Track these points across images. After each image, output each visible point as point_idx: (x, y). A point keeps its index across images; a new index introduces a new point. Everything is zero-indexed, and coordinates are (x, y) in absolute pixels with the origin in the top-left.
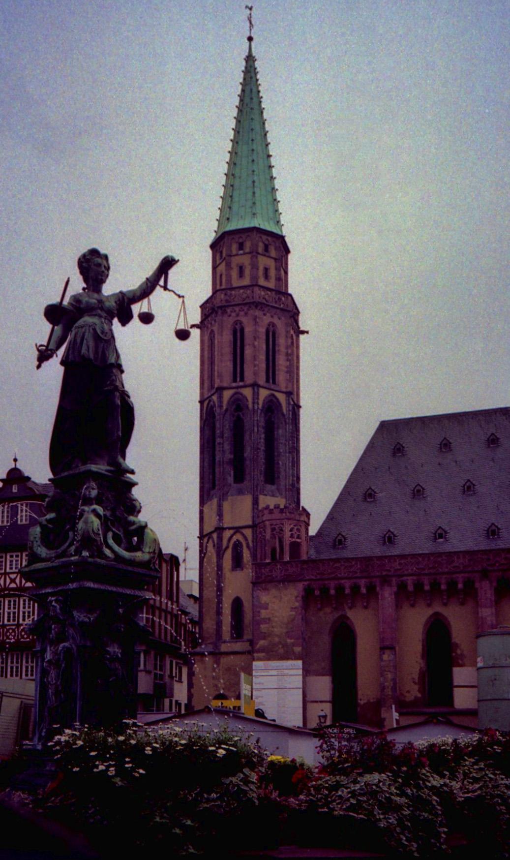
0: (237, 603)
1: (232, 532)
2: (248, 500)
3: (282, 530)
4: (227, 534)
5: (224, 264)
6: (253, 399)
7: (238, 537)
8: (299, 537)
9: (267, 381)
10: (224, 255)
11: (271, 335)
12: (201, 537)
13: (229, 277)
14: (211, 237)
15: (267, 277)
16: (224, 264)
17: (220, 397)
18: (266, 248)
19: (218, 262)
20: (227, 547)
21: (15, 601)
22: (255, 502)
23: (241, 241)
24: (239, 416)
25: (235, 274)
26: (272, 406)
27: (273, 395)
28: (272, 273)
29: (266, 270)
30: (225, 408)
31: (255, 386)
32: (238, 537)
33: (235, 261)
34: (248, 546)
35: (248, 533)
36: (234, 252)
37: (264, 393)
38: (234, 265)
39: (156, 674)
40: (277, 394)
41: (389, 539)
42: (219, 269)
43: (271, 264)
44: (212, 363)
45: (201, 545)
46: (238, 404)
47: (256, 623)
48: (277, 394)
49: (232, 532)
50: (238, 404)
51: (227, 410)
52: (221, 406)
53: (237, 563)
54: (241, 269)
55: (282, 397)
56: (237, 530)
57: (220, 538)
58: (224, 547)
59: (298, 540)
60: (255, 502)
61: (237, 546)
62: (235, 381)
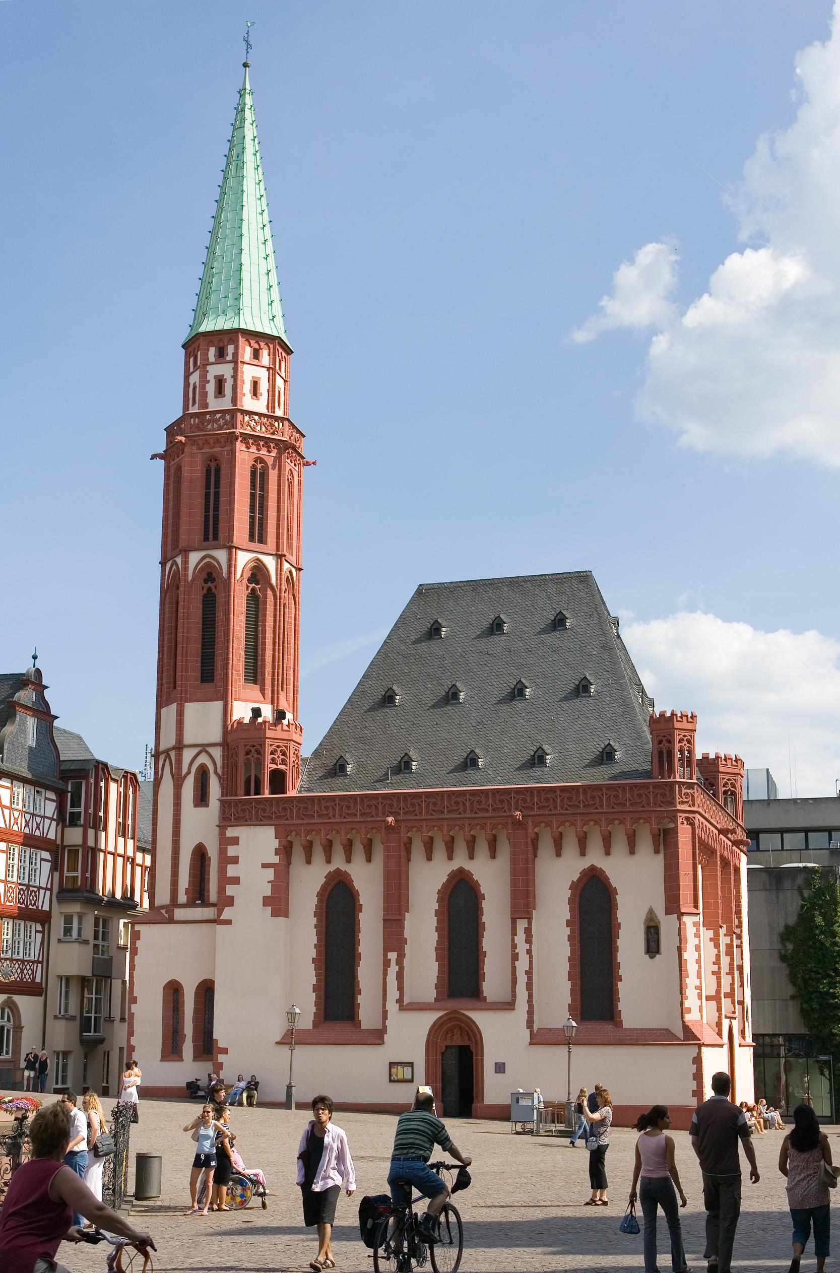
0: (200, 854)
1: (195, 751)
4: (188, 754)
5: (197, 373)
6: (229, 566)
8: (283, 762)
9: (252, 538)
11: (259, 477)
12: (156, 755)
13: (204, 394)
14: (184, 335)
15: (255, 392)
16: (197, 373)
17: (186, 563)
18: (256, 354)
19: (191, 370)
20: (189, 773)
22: (226, 712)
23: (221, 345)
24: (209, 589)
25: (211, 388)
26: (258, 573)
27: (258, 559)
28: (264, 387)
29: (255, 384)
30: (190, 577)
32: (203, 759)
33: (214, 371)
34: (216, 772)
35: (217, 753)
36: (212, 359)
37: (243, 559)
38: (210, 377)
39: (95, 946)
40: (263, 558)
43: (263, 375)
44: (177, 515)
47: (225, 880)
48: (263, 558)
49: (195, 751)
52: (186, 575)
53: (202, 799)
54: (220, 382)
55: (270, 563)
56: (203, 748)
57: (179, 761)
58: (185, 770)
59: (283, 767)
62: (206, 539)
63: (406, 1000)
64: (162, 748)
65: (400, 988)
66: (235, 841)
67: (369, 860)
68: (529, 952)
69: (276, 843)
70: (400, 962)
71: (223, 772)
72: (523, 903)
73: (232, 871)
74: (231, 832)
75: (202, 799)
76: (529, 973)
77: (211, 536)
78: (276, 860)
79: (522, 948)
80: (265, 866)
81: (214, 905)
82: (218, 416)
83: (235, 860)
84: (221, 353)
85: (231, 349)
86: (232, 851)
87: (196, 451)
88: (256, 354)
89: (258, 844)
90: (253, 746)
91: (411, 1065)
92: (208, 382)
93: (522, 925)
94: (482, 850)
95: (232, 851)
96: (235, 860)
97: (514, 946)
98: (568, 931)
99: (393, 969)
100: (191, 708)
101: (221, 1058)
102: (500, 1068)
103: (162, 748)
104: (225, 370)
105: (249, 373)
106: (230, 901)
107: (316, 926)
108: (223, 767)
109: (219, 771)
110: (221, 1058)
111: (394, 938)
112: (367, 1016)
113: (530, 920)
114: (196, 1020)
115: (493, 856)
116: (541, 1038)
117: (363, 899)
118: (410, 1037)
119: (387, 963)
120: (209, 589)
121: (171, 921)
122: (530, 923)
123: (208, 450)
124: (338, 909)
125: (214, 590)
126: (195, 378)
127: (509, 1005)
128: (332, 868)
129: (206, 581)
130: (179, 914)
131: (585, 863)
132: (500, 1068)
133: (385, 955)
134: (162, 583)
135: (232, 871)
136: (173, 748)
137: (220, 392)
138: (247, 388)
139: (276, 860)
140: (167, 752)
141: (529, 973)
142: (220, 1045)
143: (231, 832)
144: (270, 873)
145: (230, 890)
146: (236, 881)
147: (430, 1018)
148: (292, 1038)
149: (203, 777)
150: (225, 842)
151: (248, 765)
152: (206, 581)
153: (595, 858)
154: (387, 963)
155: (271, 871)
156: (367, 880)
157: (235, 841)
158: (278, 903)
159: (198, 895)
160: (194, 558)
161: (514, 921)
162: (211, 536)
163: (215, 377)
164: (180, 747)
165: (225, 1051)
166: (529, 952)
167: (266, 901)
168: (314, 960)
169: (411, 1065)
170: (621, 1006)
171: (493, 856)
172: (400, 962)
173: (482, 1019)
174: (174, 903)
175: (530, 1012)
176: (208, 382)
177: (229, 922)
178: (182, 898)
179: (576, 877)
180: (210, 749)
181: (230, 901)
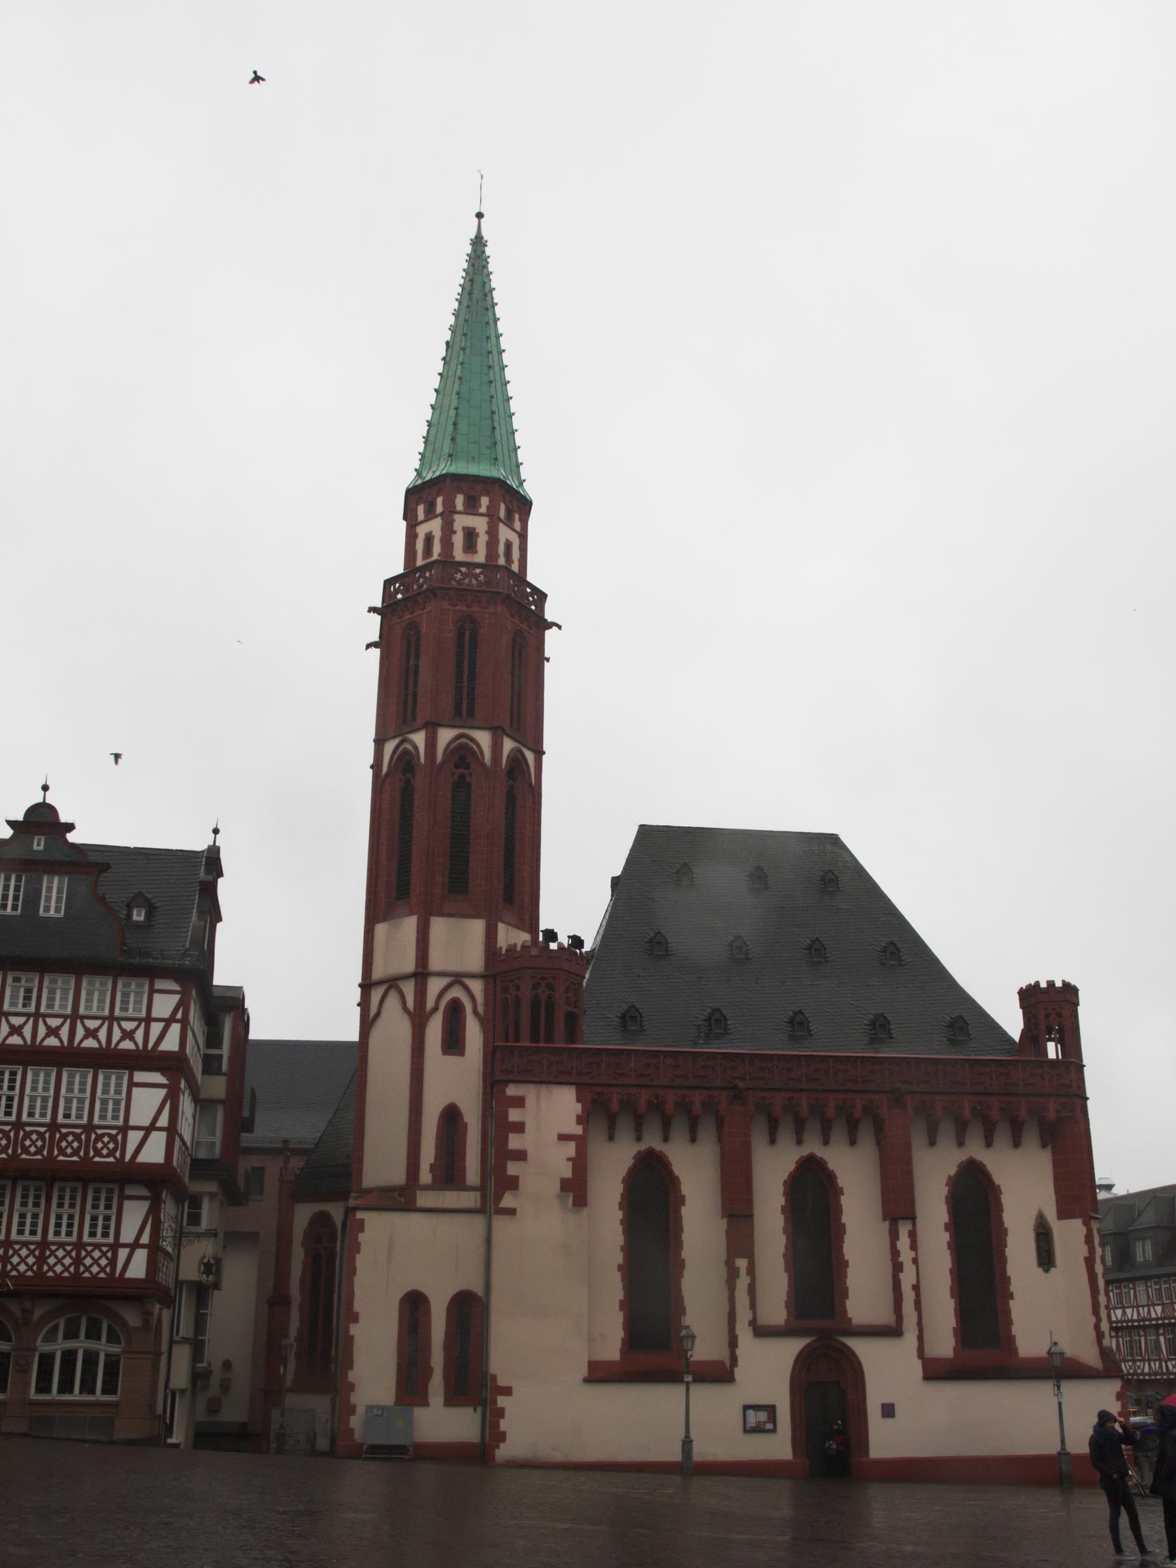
0: (451, 1116)
2: (476, 928)
3: (552, 988)
4: (435, 986)
7: (457, 992)
10: (439, 508)
12: (366, 986)
13: (447, 544)
14: (408, 478)
17: (431, 742)
20: (436, 1009)
21: (13, 1073)
25: (458, 540)
29: (508, 545)
31: (498, 732)
32: (457, 992)
33: (461, 521)
34: (475, 1012)
35: (477, 987)
41: (716, 1024)
42: (422, 531)
45: (364, 1004)
46: (463, 754)
50: (463, 754)
51: (444, 762)
53: (453, 1043)
54: (470, 536)
55: (530, 756)
56: (458, 979)
57: (421, 994)
60: (491, 935)
61: (455, 1012)
63: (760, 1322)
64: (378, 973)
65: (753, 1306)
67: (693, 1140)
68: (915, 1261)
69: (578, 1108)
70: (751, 1271)
71: (486, 1011)
73: (514, 1142)
75: (453, 1043)
76: (916, 1288)
77: (464, 713)
78: (578, 1130)
79: (906, 1255)
80: (563, 1138)
81: (473, 1189)
82: (478, 571)
83: (519, 1128)
85: (485, 501)
86: (514, 1115)
87: (448, 607)
90: (543, 979)
91: (771, 1410)
92: (455, 532)
93: (904, 1230)
95: (514, 1115)
96: (519, 1128)
97: (895, 1253)
98: (946, 1236)
99: (743, 1282)
100: (438, 925)
101: (502, 1401)
102: (888, 1411)
103: (378, 973)
105: (505, 533)
106: (513, 1184)
107: (622, 1222)
108: (486, 1004)
109: (481, 1010)
110: (502, 1401)
113: (913, 1219)
114: (448, 1347)
116: (935, 1371)
117: (687, 1188)
118: (769, 1370)
120: (462, 777)
121: (409, 1206)
122: (914, 1225)
123: (465, 609)
124: (651, 1201)
125: (468, 779)
126: (435, 526)
127: (893, 1331)
128: (642, 1147)
129: (456, 766)
132: (888, 1411)
133: (730, 1264)
134: (376, 767)
135: (514, 1142)
136: (415, 975)
138: (501, 549)
139: (578, 1130)
140: (392, 983)
142: (501, 1382)
143: (512, 1090)
144: (570, 1149)
145: (512, 1169)
147: (793, 1347)
149: (455, 1012)
151: (535, 1004)
152: (456, 766)
153: (975, 1150)
154: (732, 1275)
155: (572, 1145)
157: (519, 1102)
158: (576, 1189)
159: (449, 1174)
160: (445, 736)
162: (464, 713)
163: (464, 529)
164: (421, 975)
165: (507, 1391)
166: (915, 1261)
167: (566, 1185)
168: (620, 1268)
169: (771, 1410)
170: (1016, 1330)
172: (751, 1271)
173: (859, 1346)
175: (920, 1338)
176: (455, 532)
177: (512, 1212)
179: (952, 1171)
181: (513, 1184)
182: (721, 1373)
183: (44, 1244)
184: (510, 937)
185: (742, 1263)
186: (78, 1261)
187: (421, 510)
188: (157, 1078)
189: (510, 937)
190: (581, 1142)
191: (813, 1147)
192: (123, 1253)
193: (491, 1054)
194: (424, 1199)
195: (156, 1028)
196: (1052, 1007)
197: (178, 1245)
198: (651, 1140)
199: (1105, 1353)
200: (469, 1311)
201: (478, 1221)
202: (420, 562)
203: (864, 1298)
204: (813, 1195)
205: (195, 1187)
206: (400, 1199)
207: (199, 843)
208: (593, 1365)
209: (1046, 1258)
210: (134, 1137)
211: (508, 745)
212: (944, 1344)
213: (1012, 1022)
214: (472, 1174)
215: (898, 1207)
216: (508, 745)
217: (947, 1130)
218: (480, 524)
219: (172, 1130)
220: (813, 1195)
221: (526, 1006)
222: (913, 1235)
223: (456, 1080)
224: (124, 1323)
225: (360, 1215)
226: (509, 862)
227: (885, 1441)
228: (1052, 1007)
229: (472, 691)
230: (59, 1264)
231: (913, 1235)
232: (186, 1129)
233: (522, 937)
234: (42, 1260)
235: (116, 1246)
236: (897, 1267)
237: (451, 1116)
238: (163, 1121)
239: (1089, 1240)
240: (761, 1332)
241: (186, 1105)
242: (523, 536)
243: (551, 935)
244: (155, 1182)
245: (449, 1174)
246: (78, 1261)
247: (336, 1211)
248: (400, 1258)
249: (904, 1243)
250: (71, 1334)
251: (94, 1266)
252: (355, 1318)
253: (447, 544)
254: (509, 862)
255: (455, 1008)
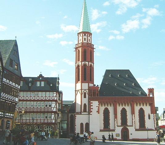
0: (85, 104)
4: (83, 91)
18: (89, 36)
22: (89, 85)
25: (84, 39)
26: (91, 65)
29: (89, 39)
31: (89, 62)
32: (85, 91)
35: (87, 91)
46: (85, 65)
50: (85, 65)
53: (85, 97)
54: (85, 39)
55: (92, 64)
56: (85, 90)
60: (89, 85)
61: (85, 93)
66: (92, 103)
70: (117, 120)
72: (133, 112)
74: (91, 102)
75: (85, 97)
76: (135, 121)
79: (134, 118)
83: (92, 106)
84: (85, 35)
85: (86, 34)
86: (91, 104)
88: (89, 36)
89: (95, 104)
93: (133, 115)
94: (126, 105)
95: (91, 104)
96: (92, 106)
99: (116, 121)
102: (131, 134)
103: (77, 90)
104: (86, 37)
105: (89, 38)
106: (92, 111)
111: (116, 117)
112: (111, 127)
115: (128, 106)
116: (136, 130)
118: (119, 130)
119: (115, 120)
130: (82, 113)
131: (140, 107)
132: (131, 134)
133: (115, 119)
137: (85, 40)
138: (89, 40)
140: (78, 91)
141: (135, 121)
143: (91, 102)
145: (91, 110)
146: (92, 109)
148: (101, 131)
150: (89, 103)
151: (93, 93)
154: (115, 120)
156: (111, 109)
157: (92, 103)
158: (98, 112)
159: (85, 111)
160: (83, 63)
161: (132, 114)
167: (97, 112)
171: (128, 106)
172: (117, 120)
174: (81, 112)
178: (82, 111)
180: (86, 90)
181: (92, 111)
182: (114, 130)
183: (44, 119)
184: (91, 85)
185: (116, 119)
186: (48, 121)
187: (79, 35)
188: (54, 102)
189: (91, 85)
190: (99, 107)
191: (124, 107)
192: (52, 120)
193: (89, 98)
194: (82, 113)
195: (54, 97)
196: (151, 91)
197: (57, 119)
198: (106, 106)
199: (155, 128)
200: (88, 125)
201: (88, 115)
202: (80, 42)
203: (129, 123)
204: (124, 112)
205: (58, 112)
206: (80, 113)
207: (57, 76)
208: (100, 130)
209: (149, 118)
210: (53, 108)
211: (90, 63)
212: (138, 127)
213: (147, 92)
214: (87, 111)
215: (133, 112)
216: (90, 63)
217: (138, 105)
218: (86, 37)
219: (56, 107)
220: (124, 112)
221: (93, 92)
222: (134, 116)
223: (86, 101)
224: (52, 126)
225: (76, 115)
226: (90, 76)
227: (131, 137)
228: (151, 91)
229: (86, 57)
230: (46, 121)
231: (134, 116)
232: (57, 107)
233: (92, 85)
234: (44, 121)
235: (51, 119)
236: (133, 120)
237: (85, 104)
238: (55, 107)
239: (154, 116)
240: (118, 126)
241: (57, 104)
242: (91, 38)
243: (95, 85)
244: (55, 112)
245: (85, 111)
246: (48, 121)
247: (73, 114)
248: (80, 119)
249: (133, 117)
250: (47, 128)
251: (49, 121)
252: (76, 126)
253: (83, 40)
254: (90, 76)
255: (85, 93)
